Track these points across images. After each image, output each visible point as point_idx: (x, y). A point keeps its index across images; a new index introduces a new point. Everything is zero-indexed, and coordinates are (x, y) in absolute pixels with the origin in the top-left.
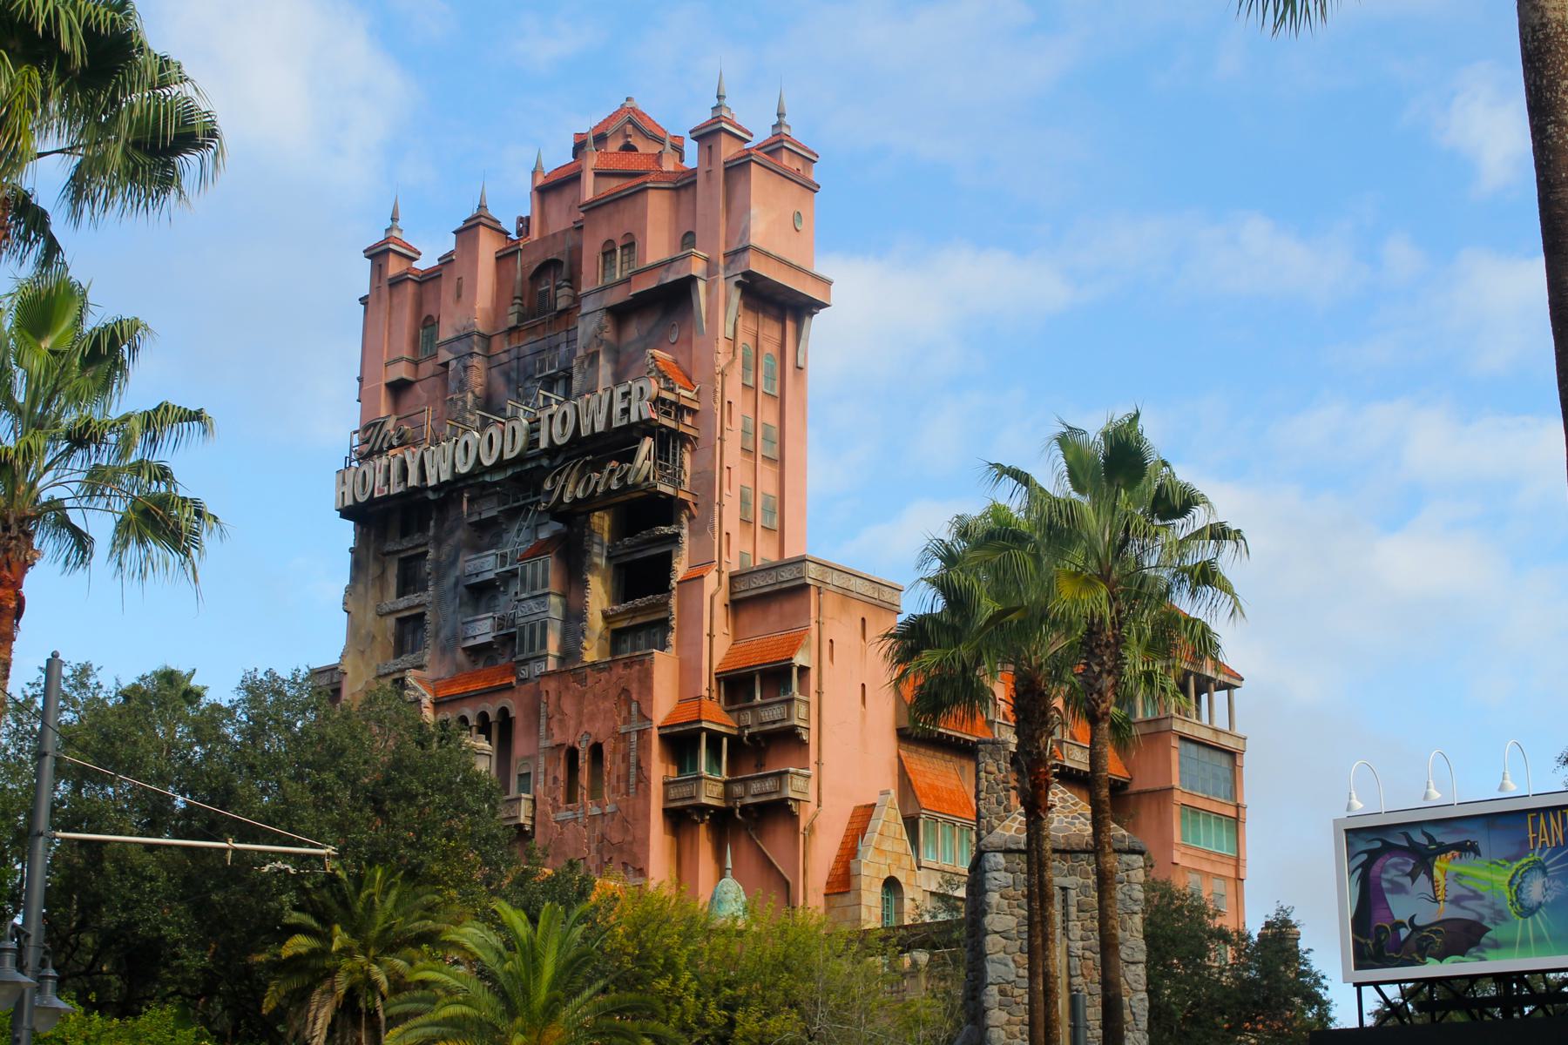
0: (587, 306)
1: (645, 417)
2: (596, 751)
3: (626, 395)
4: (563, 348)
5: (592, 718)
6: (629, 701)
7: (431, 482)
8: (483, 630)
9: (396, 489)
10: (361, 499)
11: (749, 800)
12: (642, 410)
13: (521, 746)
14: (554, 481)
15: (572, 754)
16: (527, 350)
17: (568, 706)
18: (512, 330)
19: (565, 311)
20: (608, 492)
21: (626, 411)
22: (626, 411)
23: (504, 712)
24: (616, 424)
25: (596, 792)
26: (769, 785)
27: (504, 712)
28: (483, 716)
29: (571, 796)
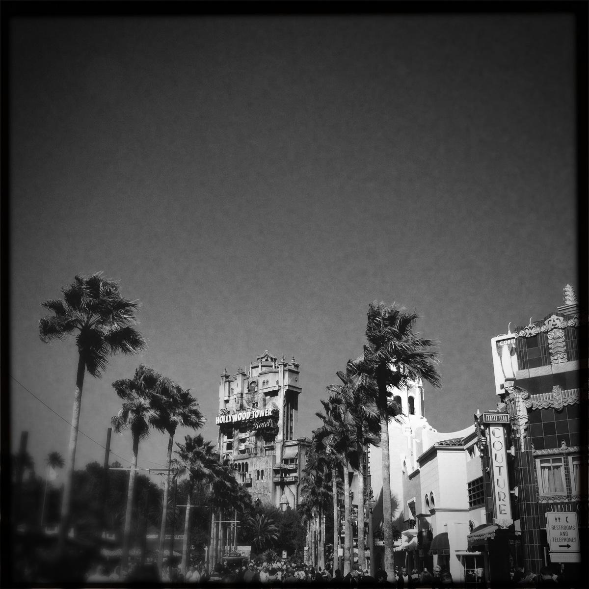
0: (260, 392)
1: (271, 414)
2: (262, 471)
3: (267, 411)
4: (256, 398)
5: (262, 465)
6: (268, 463)
7: (234, 421)
8: (242, 447)
9: (227, 421)
10: (221, 422)
11: (288, 481)
12: (270, 414)
13: (250, 469)
14: (255, 424)
15: (258, 471)
16: (250, 397)
17: (258, 463)
18: (247, 393)
19: (257, 391)
20: (264, 427)
21: (267, 413)
22: (267, 413)
23: (247, 463)
24: (266, 415)
25: (262, 478)
26: (291, 478)
27: (247, 463)
28: (243, 463)
29: (258, 479)
